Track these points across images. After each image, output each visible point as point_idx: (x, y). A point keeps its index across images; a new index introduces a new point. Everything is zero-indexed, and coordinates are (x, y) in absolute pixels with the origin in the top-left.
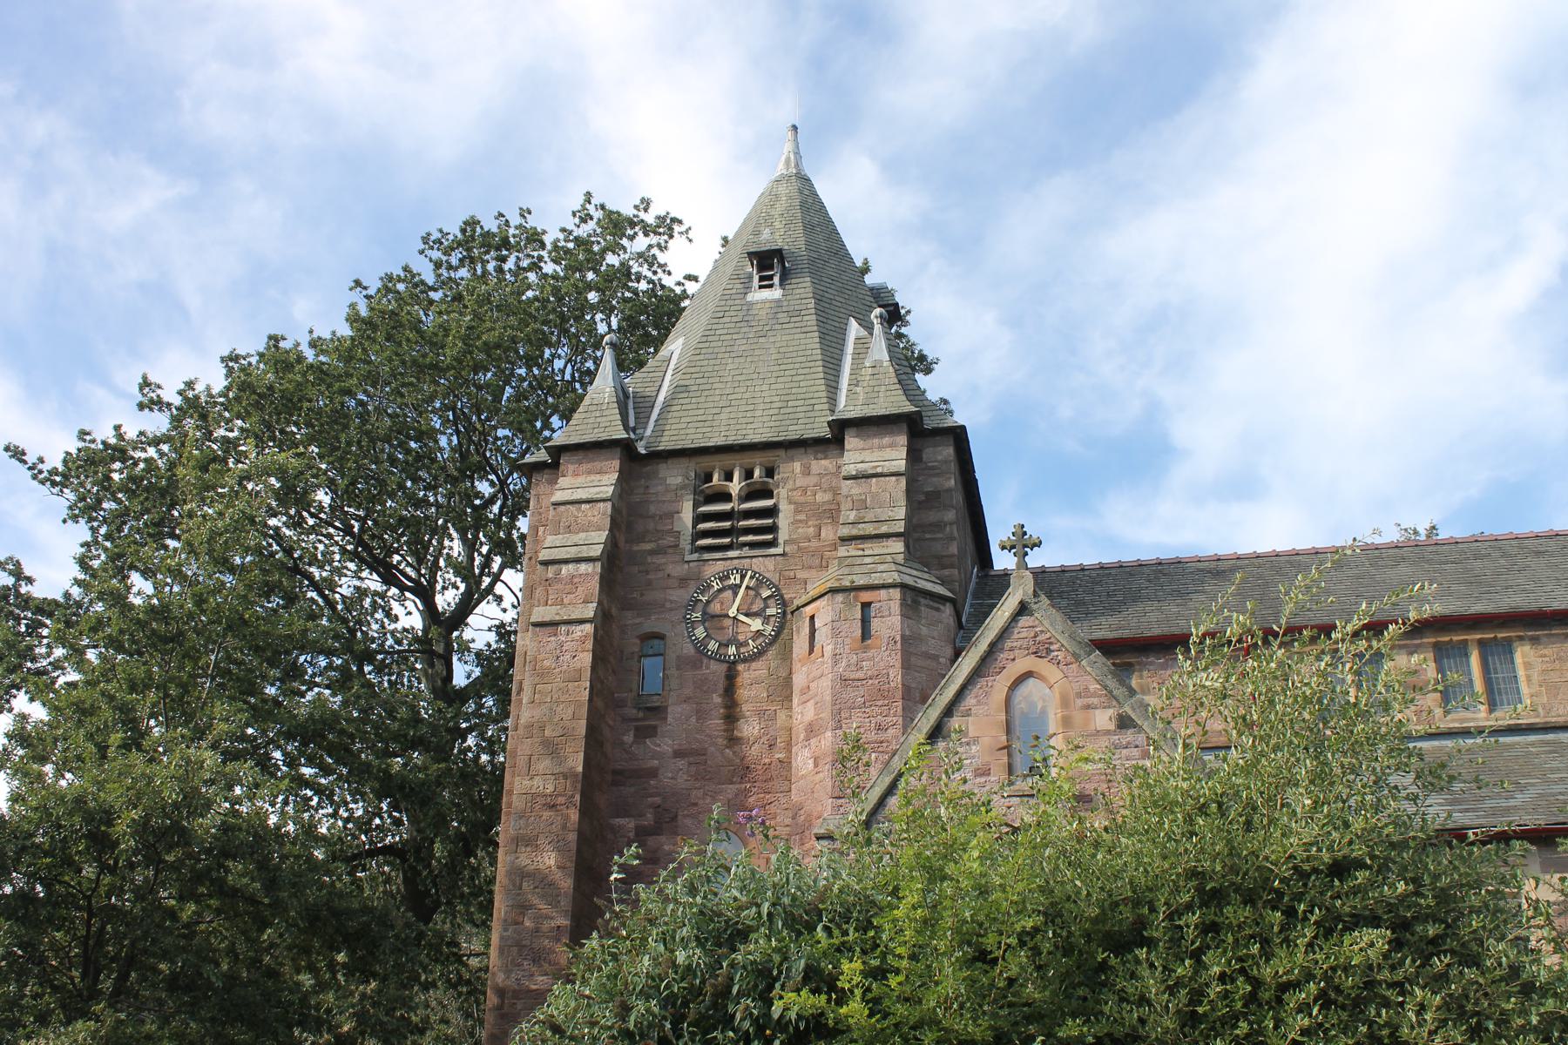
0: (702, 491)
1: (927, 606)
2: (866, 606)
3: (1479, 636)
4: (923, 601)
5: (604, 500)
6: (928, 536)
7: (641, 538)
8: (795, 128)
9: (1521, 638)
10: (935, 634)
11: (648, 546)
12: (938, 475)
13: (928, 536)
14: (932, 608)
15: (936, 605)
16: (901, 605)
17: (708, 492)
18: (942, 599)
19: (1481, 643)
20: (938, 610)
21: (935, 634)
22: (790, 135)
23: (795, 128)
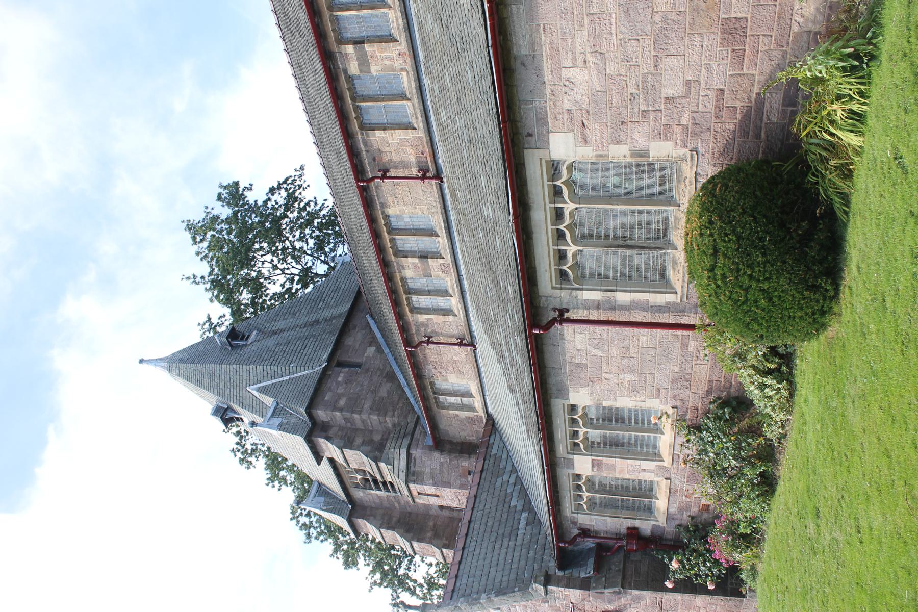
0: (364, 485)
1: (414, 467)
2: (419, 493)
3: (386, 234)
4: (412, 469)
5: (380, 531)
6: (370, 424)
7: (394, 506)
8: (141, 361)
9: (383, 213)
10: (428, 463)
11: (396, 505)
12: (335, 418)
13: (370, 424)
14: (415, 463)
15: (413, 460)
16: (417, 484)
17: (363, 483)
18: (409, 455)
19: (389, 233)
20: (415, 459)
21: (428, 463)
22: (145, 365)
23: (141, 361)
